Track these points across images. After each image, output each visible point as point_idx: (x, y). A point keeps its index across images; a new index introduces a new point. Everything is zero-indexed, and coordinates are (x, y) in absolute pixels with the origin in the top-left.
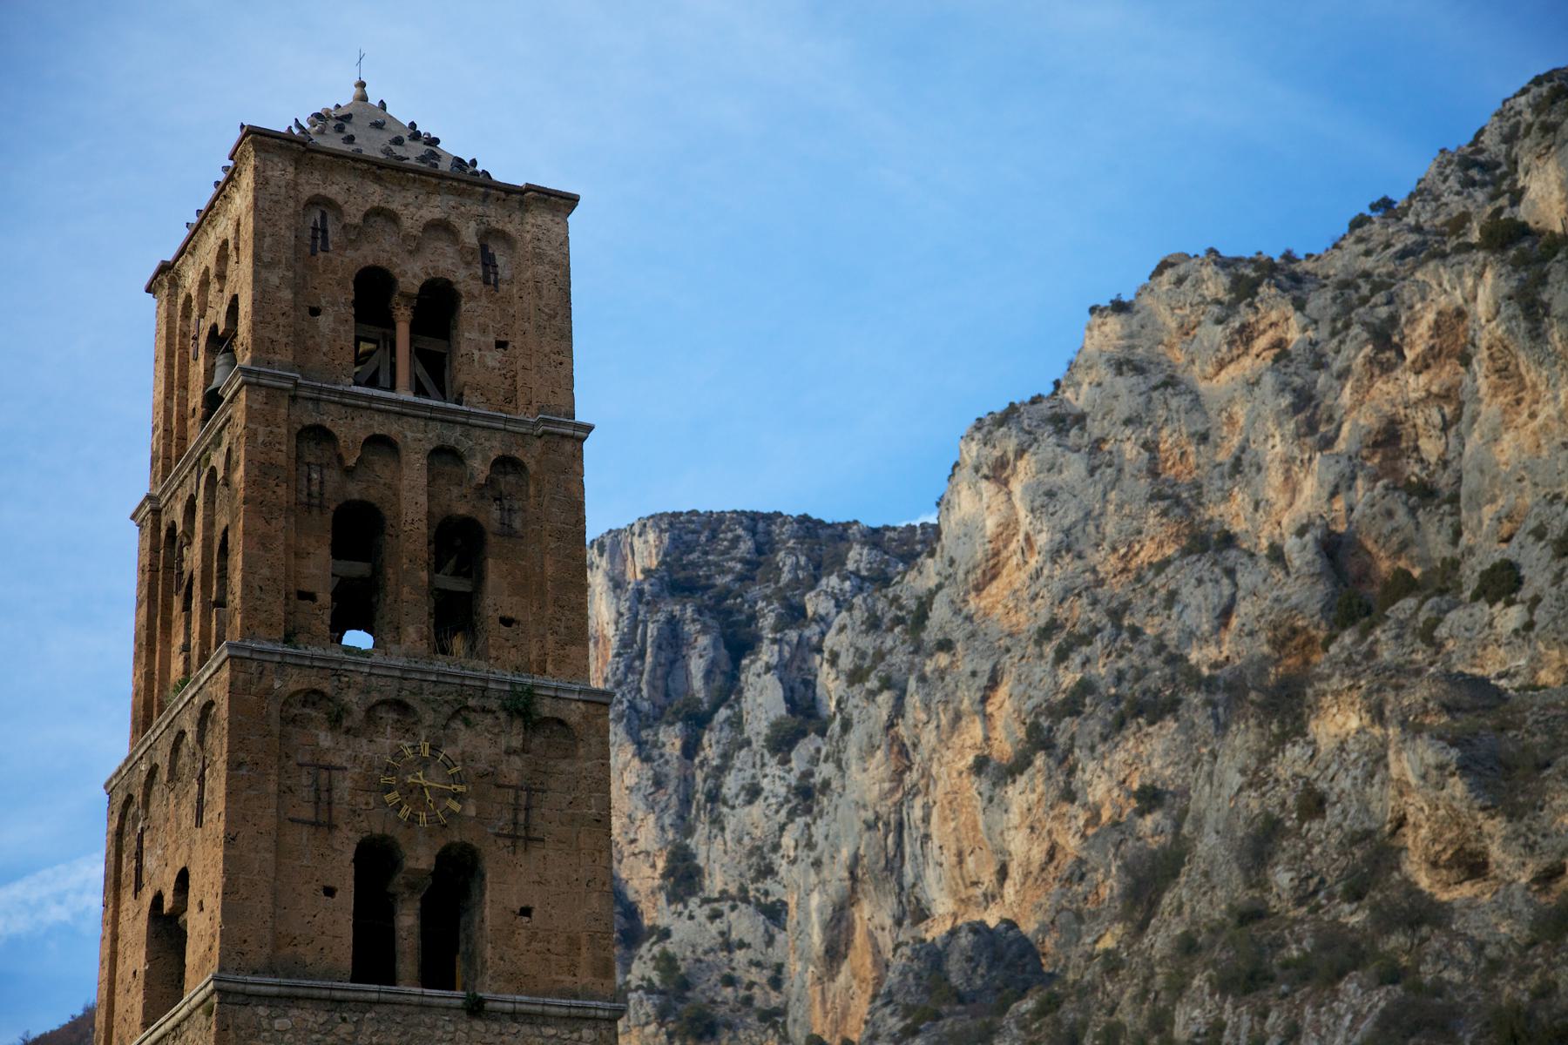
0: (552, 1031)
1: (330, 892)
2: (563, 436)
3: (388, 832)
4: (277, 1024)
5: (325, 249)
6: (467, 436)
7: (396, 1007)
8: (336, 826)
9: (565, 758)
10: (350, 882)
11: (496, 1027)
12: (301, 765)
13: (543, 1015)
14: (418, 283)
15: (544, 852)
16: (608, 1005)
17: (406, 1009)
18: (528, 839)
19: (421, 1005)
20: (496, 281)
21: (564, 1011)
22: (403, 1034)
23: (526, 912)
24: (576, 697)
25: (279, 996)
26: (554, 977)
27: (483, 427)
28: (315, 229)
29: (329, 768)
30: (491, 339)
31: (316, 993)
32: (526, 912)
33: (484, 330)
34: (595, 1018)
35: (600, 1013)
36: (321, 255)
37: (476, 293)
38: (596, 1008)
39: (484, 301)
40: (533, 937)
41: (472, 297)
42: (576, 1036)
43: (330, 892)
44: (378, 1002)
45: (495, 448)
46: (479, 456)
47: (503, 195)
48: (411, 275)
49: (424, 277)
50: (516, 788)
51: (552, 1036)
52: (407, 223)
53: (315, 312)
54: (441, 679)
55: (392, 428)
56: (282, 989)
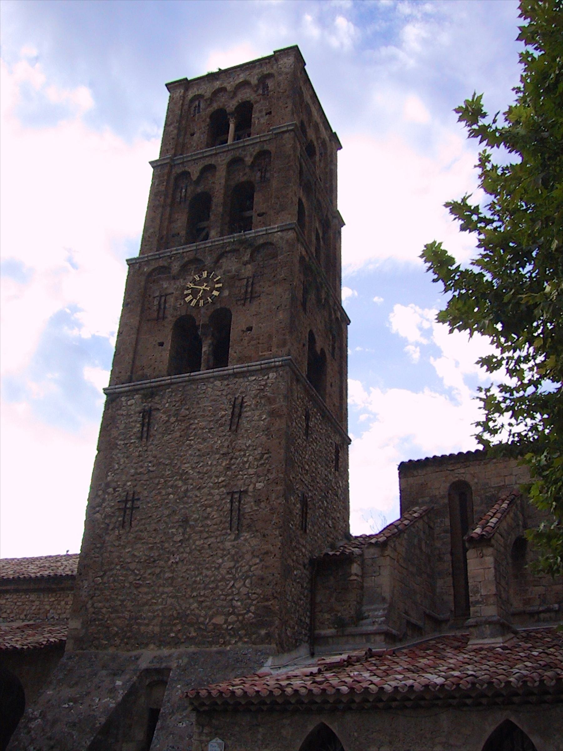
0: (254, 378)
1: (161, 344)
2: (284, 132)
3: (188, 313)
4: (129, 403)
5: (199, 112)
6: (244, 151)
7: (180, 384)
8: (166, 318)
9: (273, 258)
10: (170, 337)
11: (226, 382)
12: (154, 298)
13: (248, 371)
14: (234, 108)
15: (259, 301)
16: (281, 359)
17: (184, 384)
18: (252, 298)
19: (189, 381)
20: (268, 92)
21: (258, 367)
22: (182, 395)
23: (250, 329)
24: (276, 230)
25: (129, 391)
26: (261, 354)
27: (251, 144)
28: (196, 107)
29: (166, 295)
30: (264, 113)
31: (144, 386)
32: (250, 329)
33: (260, 111)
34: (275, 367)
35: (277, 363)
36: (197, 115)
37: (258, 100)
38: (275, 362)
39: (262, 102)
40: (252, 339)
41: (256, 102)
42: (266, 377)
43: (161, 344)
44: (172, 384)
45: (257, 148)
46: (249, 156)
47: (267, 61)
48: (232, 105)
49: (237, 104)
50: (248, 278)
51: (254, 380)
52: (229, 88)
53: (192, 135)
54: (213, 244)
55: (213, 161)
56: (130, 387)
